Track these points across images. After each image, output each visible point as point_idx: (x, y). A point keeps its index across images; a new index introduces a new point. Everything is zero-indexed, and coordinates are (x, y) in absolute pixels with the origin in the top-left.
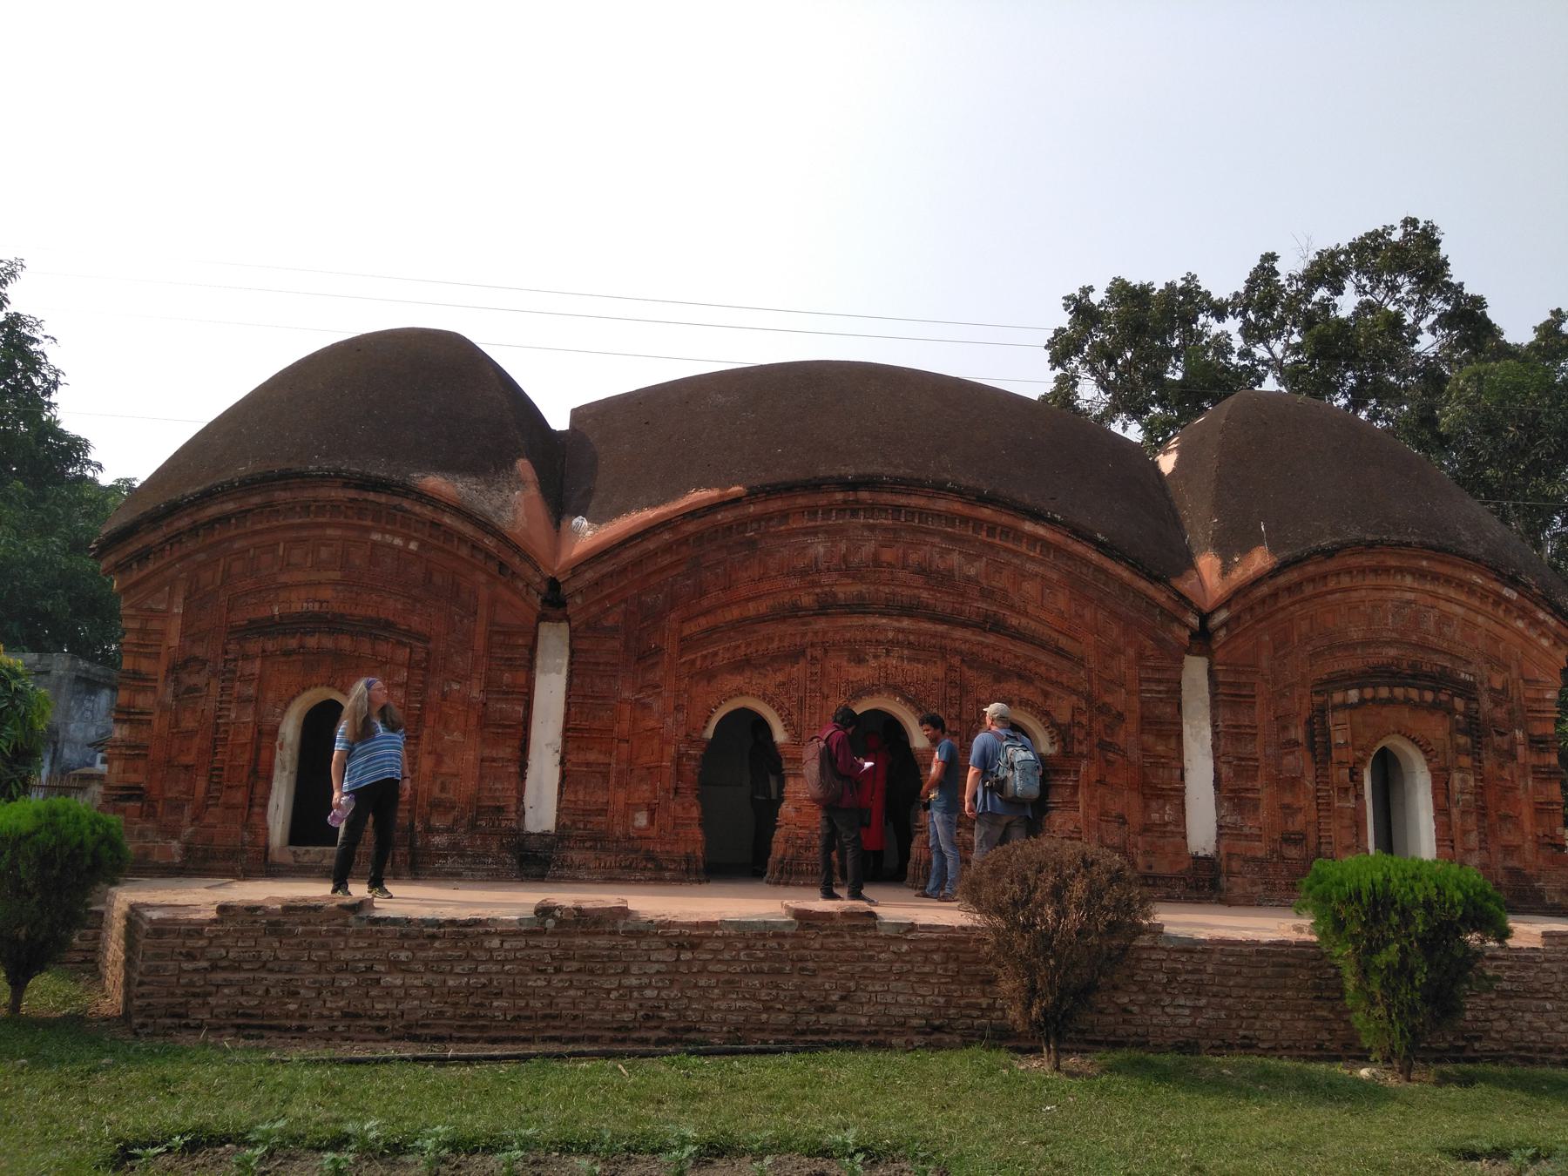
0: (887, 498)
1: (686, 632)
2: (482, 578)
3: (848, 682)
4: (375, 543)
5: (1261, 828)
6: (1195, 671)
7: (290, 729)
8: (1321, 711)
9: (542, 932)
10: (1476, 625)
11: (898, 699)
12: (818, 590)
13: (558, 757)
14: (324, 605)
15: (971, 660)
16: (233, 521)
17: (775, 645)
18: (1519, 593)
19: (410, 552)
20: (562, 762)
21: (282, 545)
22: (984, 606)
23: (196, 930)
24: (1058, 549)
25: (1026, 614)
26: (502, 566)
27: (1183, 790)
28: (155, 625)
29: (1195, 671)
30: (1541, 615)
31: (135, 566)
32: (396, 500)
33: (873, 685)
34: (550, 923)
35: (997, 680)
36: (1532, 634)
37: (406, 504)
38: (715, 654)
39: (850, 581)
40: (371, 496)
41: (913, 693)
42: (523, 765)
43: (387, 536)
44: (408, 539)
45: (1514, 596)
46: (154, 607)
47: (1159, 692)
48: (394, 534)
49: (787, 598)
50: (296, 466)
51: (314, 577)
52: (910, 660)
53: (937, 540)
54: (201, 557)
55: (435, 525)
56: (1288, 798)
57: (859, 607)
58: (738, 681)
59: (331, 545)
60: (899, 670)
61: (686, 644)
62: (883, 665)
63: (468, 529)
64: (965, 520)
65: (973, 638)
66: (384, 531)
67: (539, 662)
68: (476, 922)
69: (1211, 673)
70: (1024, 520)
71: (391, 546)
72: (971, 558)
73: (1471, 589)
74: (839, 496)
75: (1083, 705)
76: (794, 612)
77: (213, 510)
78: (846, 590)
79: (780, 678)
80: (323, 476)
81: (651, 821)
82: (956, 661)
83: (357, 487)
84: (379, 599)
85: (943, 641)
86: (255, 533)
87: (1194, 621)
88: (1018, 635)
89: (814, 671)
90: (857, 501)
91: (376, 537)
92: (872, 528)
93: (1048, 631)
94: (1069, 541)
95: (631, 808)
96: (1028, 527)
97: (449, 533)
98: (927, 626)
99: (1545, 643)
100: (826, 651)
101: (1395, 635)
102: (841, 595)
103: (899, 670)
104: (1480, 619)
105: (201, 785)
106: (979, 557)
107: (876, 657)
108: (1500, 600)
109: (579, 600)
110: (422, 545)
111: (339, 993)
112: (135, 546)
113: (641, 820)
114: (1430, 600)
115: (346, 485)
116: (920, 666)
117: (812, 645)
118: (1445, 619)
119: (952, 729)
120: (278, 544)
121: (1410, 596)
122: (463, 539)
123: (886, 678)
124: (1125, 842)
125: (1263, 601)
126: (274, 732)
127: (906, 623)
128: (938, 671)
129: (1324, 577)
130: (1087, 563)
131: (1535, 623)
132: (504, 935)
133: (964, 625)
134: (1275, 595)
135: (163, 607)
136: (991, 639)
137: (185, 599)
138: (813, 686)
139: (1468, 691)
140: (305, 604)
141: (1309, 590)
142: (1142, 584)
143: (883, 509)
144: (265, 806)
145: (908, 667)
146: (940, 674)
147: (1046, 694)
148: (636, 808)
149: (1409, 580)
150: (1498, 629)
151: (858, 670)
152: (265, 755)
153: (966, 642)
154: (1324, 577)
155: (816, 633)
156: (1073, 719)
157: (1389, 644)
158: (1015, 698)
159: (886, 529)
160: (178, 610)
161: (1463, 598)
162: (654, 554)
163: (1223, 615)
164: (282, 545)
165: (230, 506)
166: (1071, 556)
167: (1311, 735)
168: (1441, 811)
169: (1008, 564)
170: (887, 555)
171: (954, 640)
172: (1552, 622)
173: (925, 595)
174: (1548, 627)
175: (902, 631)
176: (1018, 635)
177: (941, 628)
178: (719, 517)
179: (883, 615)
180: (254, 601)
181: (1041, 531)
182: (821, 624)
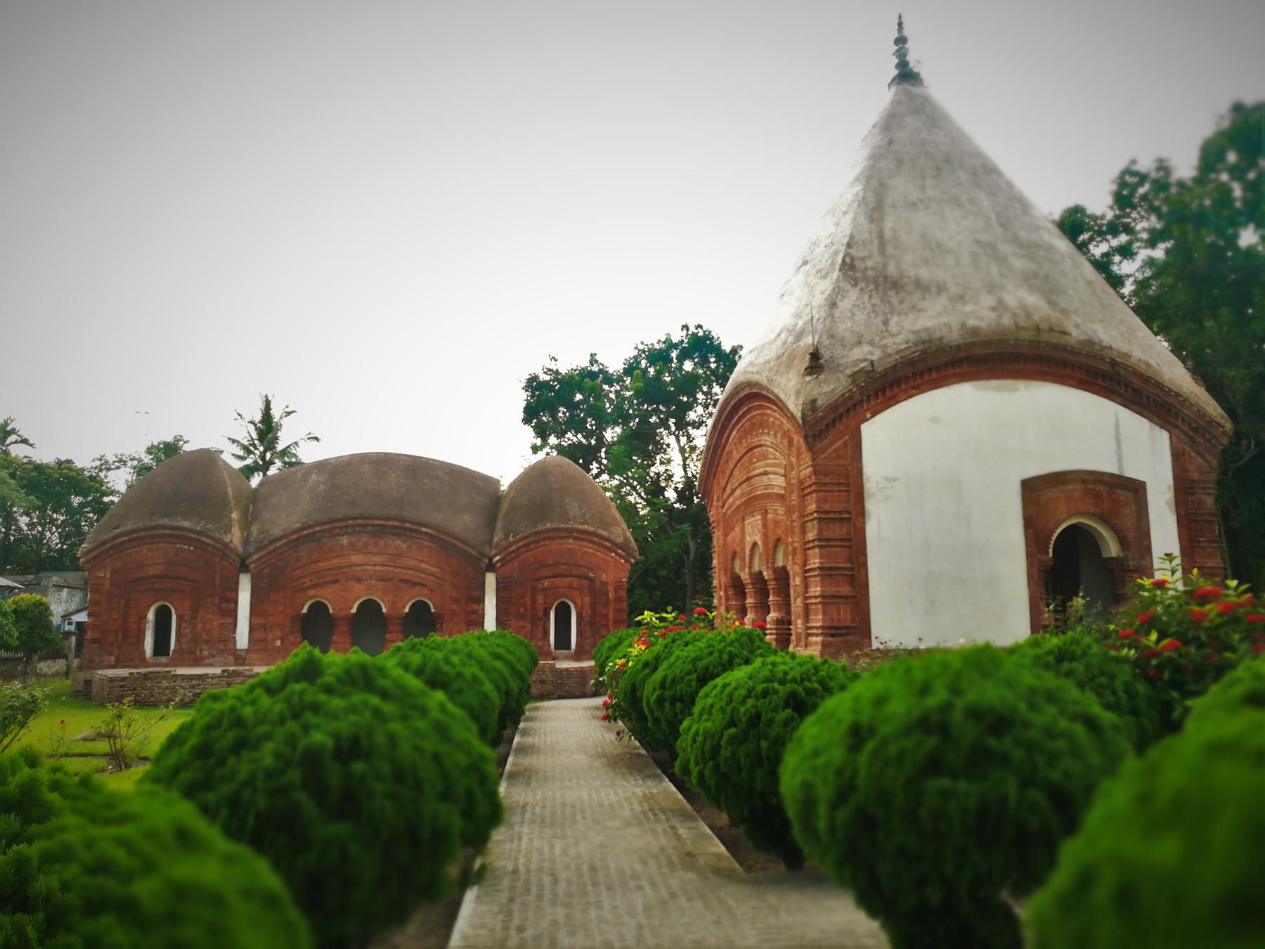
4: (179, 548)
6: (491, 580)
7: (151, 616)
9: (223, 677)
10: (596, 555)
13: (248, 622)
20: (250, 623)
23: (124, 679)
24: (435, 537)
26: (224, 554)
27: (483, 622)
29: (491, 580)
30: (619, 551)
34: (226, 674)
35: (413, 586)
36: (618, 558)
42: (235, 624)
44: (190, 546)
45: (610, 545)
51: (157, 562)
56: (521, 623)
58: (312, 592)
64: (400, 528)
67: (240, 588)
68: (204, 675)
69: (497, 579)
73: (594, 543)
81: (282, 643)
86: (135, 547)
87: (487, 561)
91: (178, 545)
95: (275, 639)
96: (424, 529)
97: (204, 543)
99: (622, 561)
101: (565, 561)
104: (599, 554)
105: (120, 637)
106: (407, 541)
108: (605, 547)
110: (195, 547)
111: (166, 695)
113: (278, 643)
118: (587, 554)
121: (572, 546)
122: (209, 545)
125: (514, 551)
126: (145, 617)
127: (378, 568)
129: (538, 541)
131: (617, 554)
132: (212, 678)
134: (519, 549)
139: (591, 580)
141: (532, 546)
143: (368, 525)
144: (143, 643)
148: (277, 639)
149: (571, 541)
150: (605, 557)
152: (142, 625)
154: (538, 541)
157: (564, 564)
161: (591, 546)
162: (280, 547)
163: (498, 558)
165: (125, 538)
166: (441, 539)
168: (578, 624)
172: (623, 553)
181: (429, 531)
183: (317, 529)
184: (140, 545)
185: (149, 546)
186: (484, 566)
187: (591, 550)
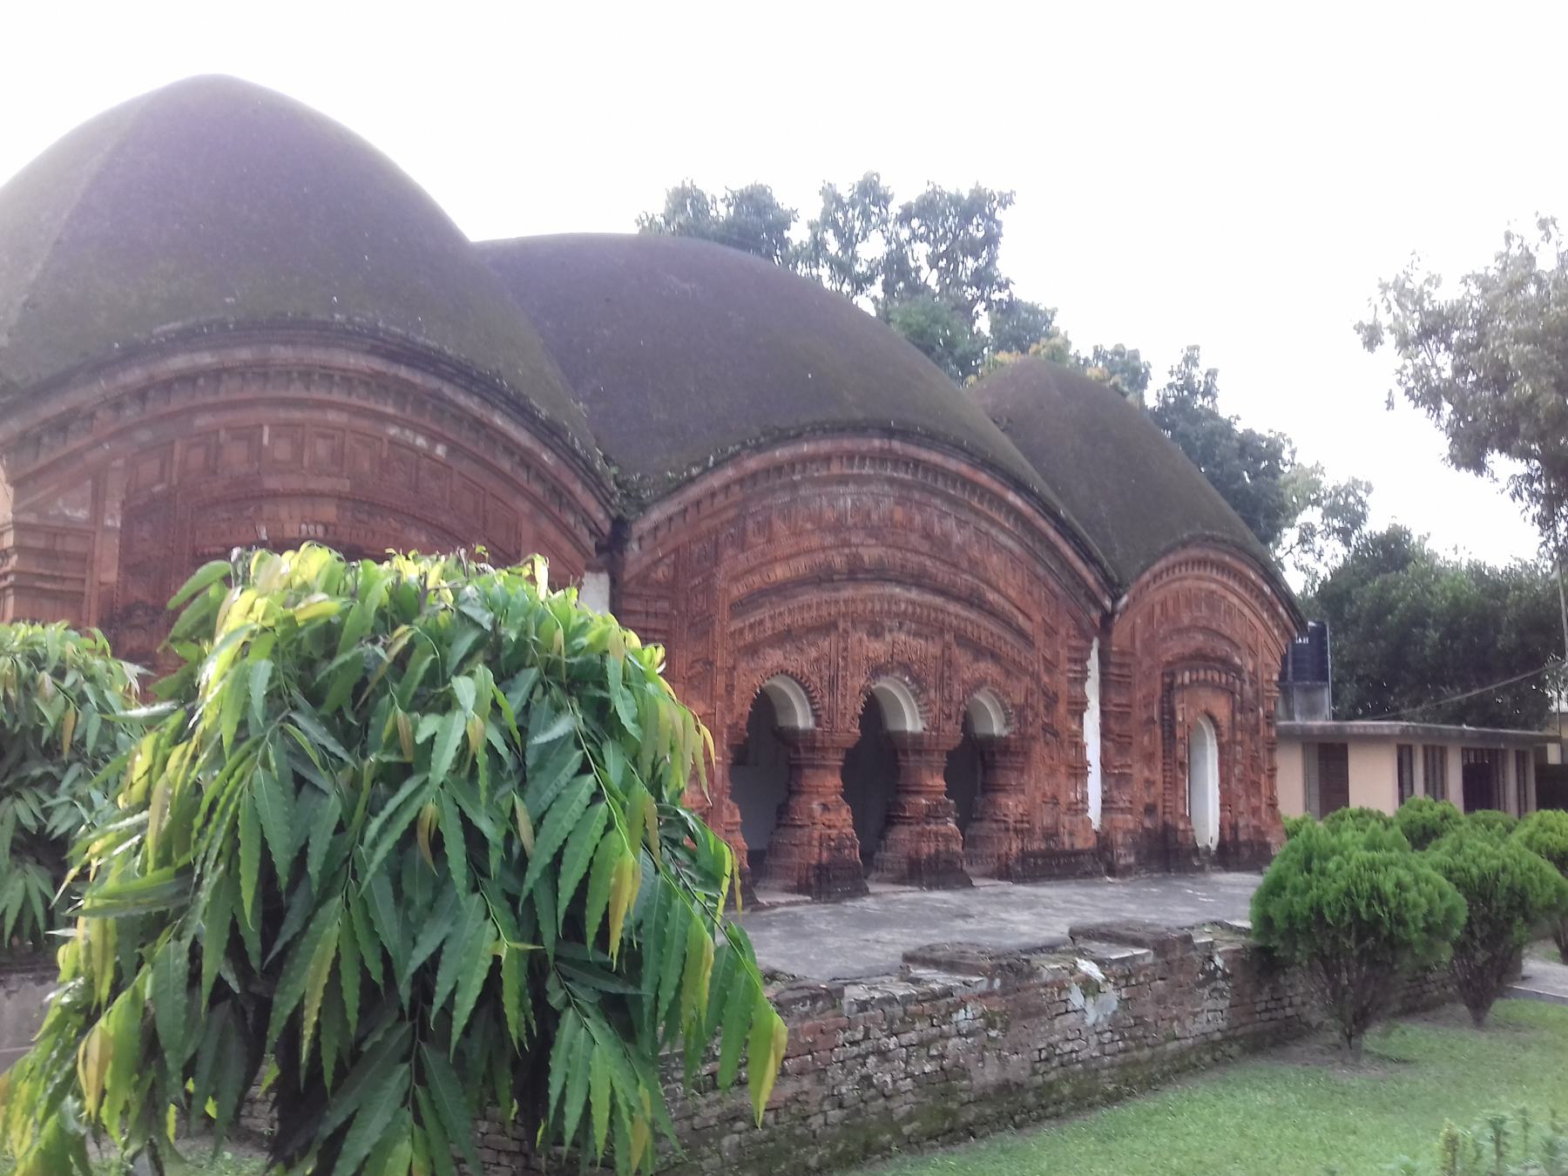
0: (913, 450)
1: (738, 590)
2: (523, 506)
3: (868, 658)
4: (393, 442)
5: (1131, 802)
8: (1169, 689)
12: (847, 551)
14: (331, 529)
15: (963, 640)
16: (201, 382)
17: (814, 613)
18: (1272, 589)
19: (435, 460)
21: (266, 430)
22: (969, 578)
25: (999, 591)
28: (72, 545)
30: (1281, 610)
31: (46, 440)
32: (434, 383)
35: (976, 660)
37: (448, 390)
38: (761, 622)
39: (873, 542)
40: (404, 372)
43: (407, 432)
44: (434, 438)
46: (67, 512)
47: (1075, 672)
48: (418, 429)
49: (820, 558)
50: (318, 316)
52: (917, 634)
53: (937, 502)
54: (144, 436)
55: (479, 425)
57: (880, 574)
58: (774, 657)
59: (332, 437)
61: (740, 607)
63: (522, 437)
66: (404, 424)
70: (1009, 488)
71: (413, 448)
72: (961, 524)
74: (877, 443)
75: (1034, 687)
76: (823, 578)
77: (180, 362)
78: (871, 553)
79: (814, 653)
80: (348, 332)
82: (949, 637)
83: (392, 357)
84: (398, 526)
86: (232, 405)
88: (992, 613)
90: (890, 451)
91: (393, 431)
92: (891, 481)
93: (1008, 606)
94: (1037, 515)
96: (1012, 497)
98: (929, 598)
102: (866, 558)
107: (891, 631)
109: (635, 546)
110: (453, 448)
112: (53, 408)
114: (1221, 591)
115: (373, 351)
117: (844, 615)
120: (261, 426)
121: (1214, 586)
122: (511, 447)
124: (1057, 824)
127: (914, 594)
128: (934, 649)
130: (1043, 537)
133: (957, 599)
135: (82, 514)
136: (973, 615)
137: (123, 503)
140: (304, 527)
142: (1079, 565)
146: (939, 653)
147: (1008, 673)
153: (957, 616)
155: (846, 602)
156: (1026, 699)
158: (989, 678)
159: (903, 484)
160: (114, 521)
164: (266, 430)
165: (206, 359)
167: (1162, 713)
168: (1224, 780)
169: (987, 534)
170: (899, 514)
172: (1285, 615)
173: (928, 563)
174: (1282, 620)
175: (913, 603)
176: (992, 613)
177: (939, 601)
178: (777, 454)
179: (899, 582)
180: (225, 515)
182: (848, 592)
183: (806, 448)
184: (251, 403)
185: (283, 414)
186: (1096, 615)
187: (1235, 601)
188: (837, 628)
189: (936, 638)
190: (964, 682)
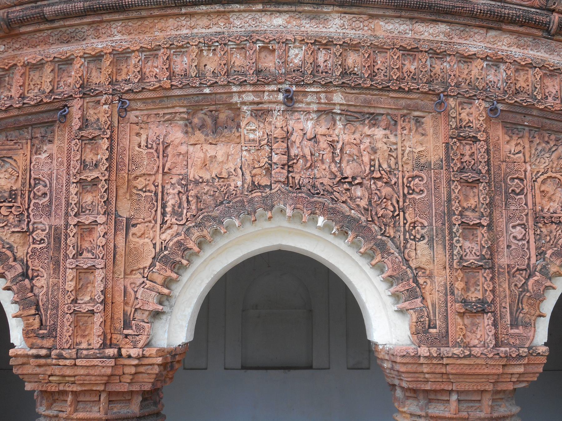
11: (321, 221)
33: (255, 187)
41: (363, 203)
60: (323, 144)
62: (278, 133)
65: (517, 53)
85: (438, 66)
89: (89, 157)
100: (124, 110)
103: (323, 144)
116: (379, 133)
119: (474, 295)
123: (289, 166)
138: (88, 198)
145: (346, 137)
151: (211, 151)
155: (97, 57)
171: (468, 59)
188: (65, 118)
189: (428, 121)
190: (539, 218)
